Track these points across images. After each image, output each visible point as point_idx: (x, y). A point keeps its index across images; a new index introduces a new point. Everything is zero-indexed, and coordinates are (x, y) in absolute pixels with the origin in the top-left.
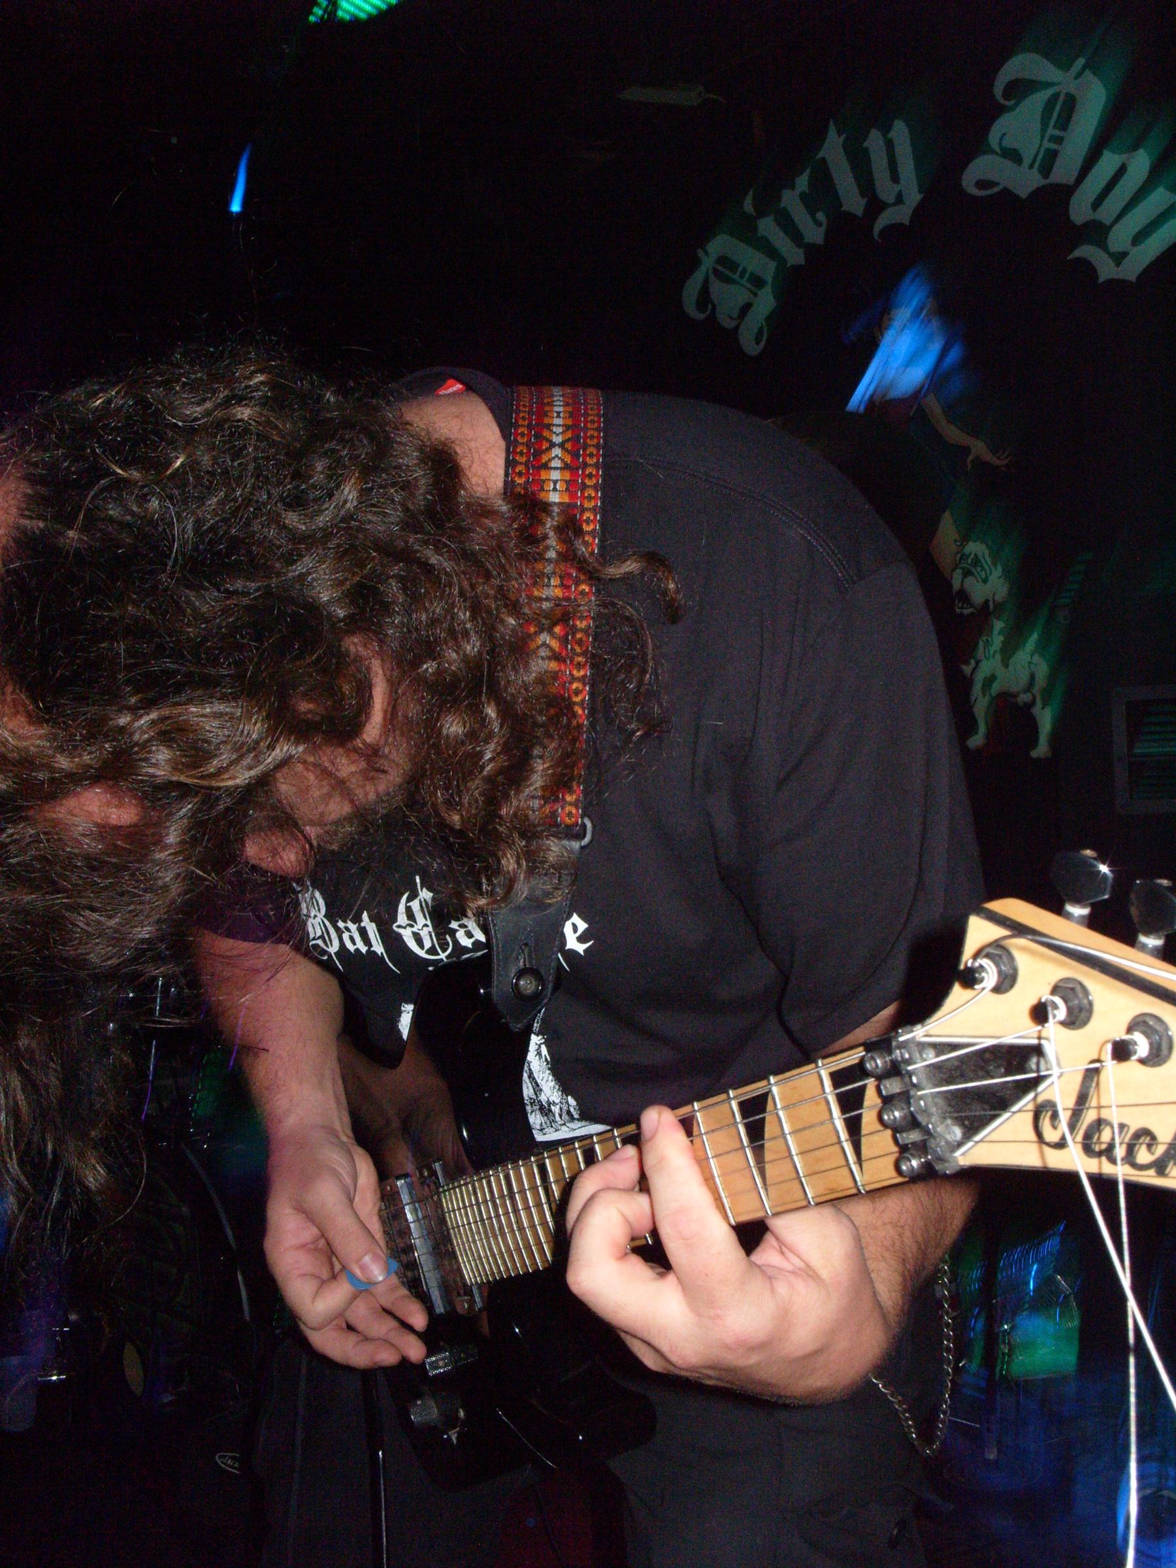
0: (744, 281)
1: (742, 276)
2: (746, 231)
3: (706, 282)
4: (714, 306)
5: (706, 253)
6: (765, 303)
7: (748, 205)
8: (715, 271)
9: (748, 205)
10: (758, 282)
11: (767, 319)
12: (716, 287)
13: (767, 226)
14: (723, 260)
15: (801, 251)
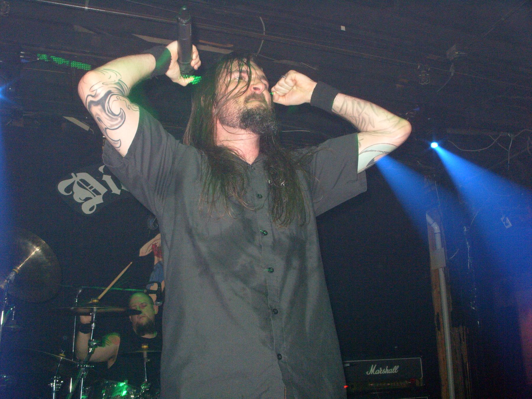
0: (91, 190)
1: (91, 188)
2: (98, 177)
3: (73, 183)
4: (73, 193)
5: (76, 176)
6: (98, 200)
7: (101, 169)
8: (78, 183)
9: (101, 169)
10: (98, 193)
11: (97, 205)
12: (76, 188)
13: (107, 178)
14: (82, 180)
15: (120, 191)
